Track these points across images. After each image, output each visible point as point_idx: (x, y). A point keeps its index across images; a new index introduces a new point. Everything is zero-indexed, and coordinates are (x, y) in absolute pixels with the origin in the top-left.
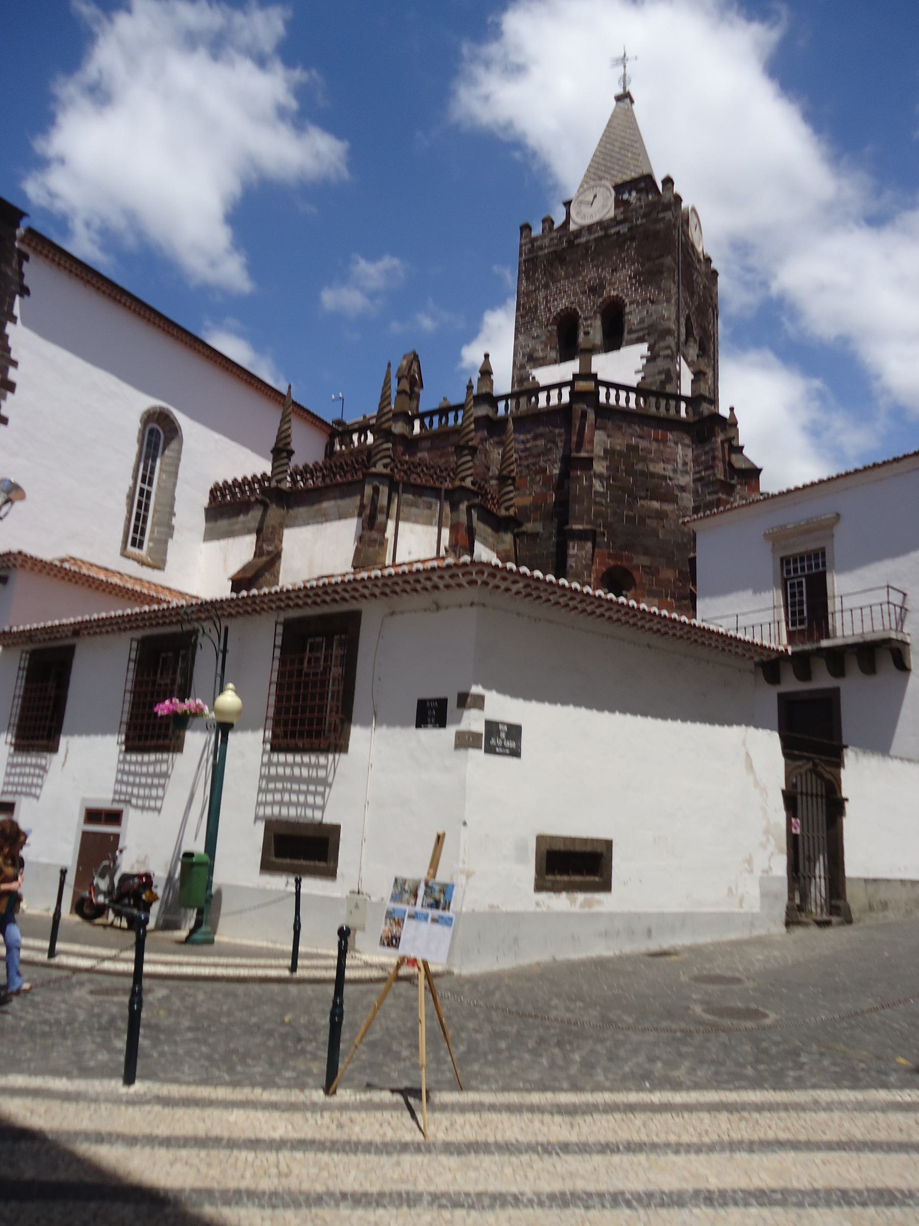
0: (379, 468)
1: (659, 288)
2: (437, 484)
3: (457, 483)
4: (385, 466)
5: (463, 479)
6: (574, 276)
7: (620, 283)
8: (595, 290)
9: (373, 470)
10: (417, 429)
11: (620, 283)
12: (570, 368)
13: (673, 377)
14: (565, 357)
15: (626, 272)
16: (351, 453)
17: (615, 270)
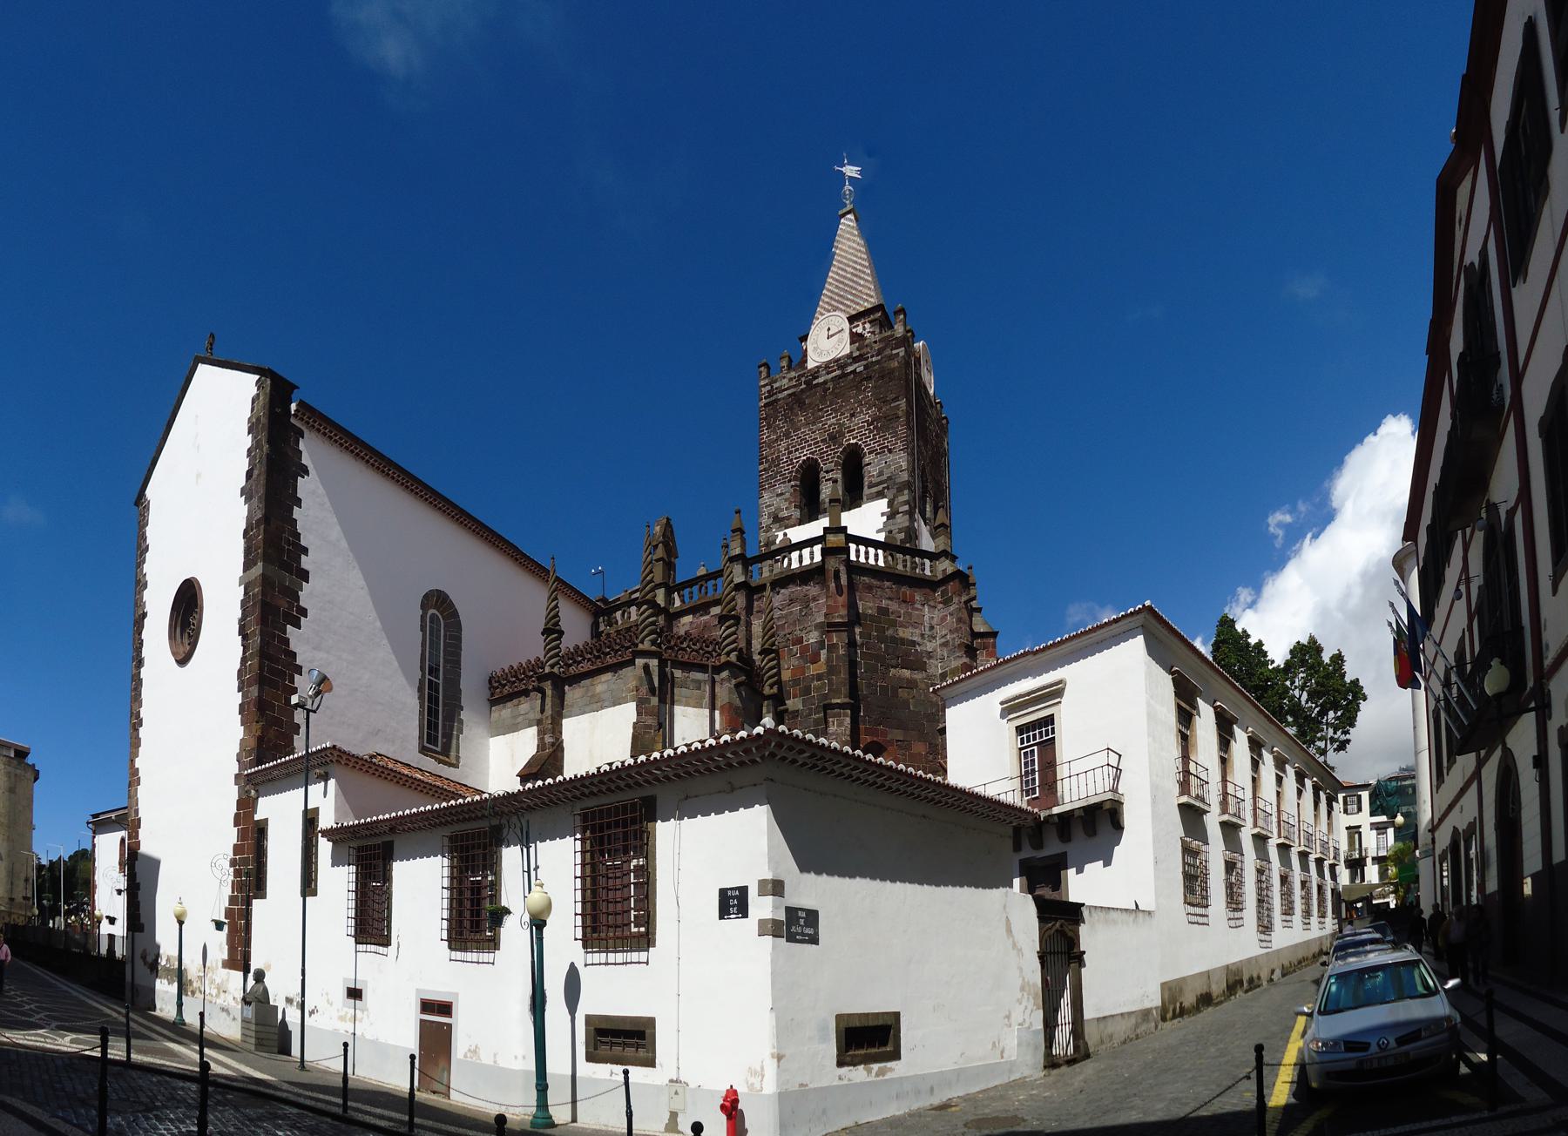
0: (646, 646)
1: (895, 434)
2: (704, 661)
3: (723, 659)
4: (653, 642)
5: (728, 654)
6: (814, 423)
7: (858, 427)
8: (834, 438)
9: (641, 647)
10: (678, 603)
11: (858, 427)
12: (815, 528)
13: (912, 534)
14: (810, 515)
15: (865, 416)
16: (618, 632)
17: (853, 415)
